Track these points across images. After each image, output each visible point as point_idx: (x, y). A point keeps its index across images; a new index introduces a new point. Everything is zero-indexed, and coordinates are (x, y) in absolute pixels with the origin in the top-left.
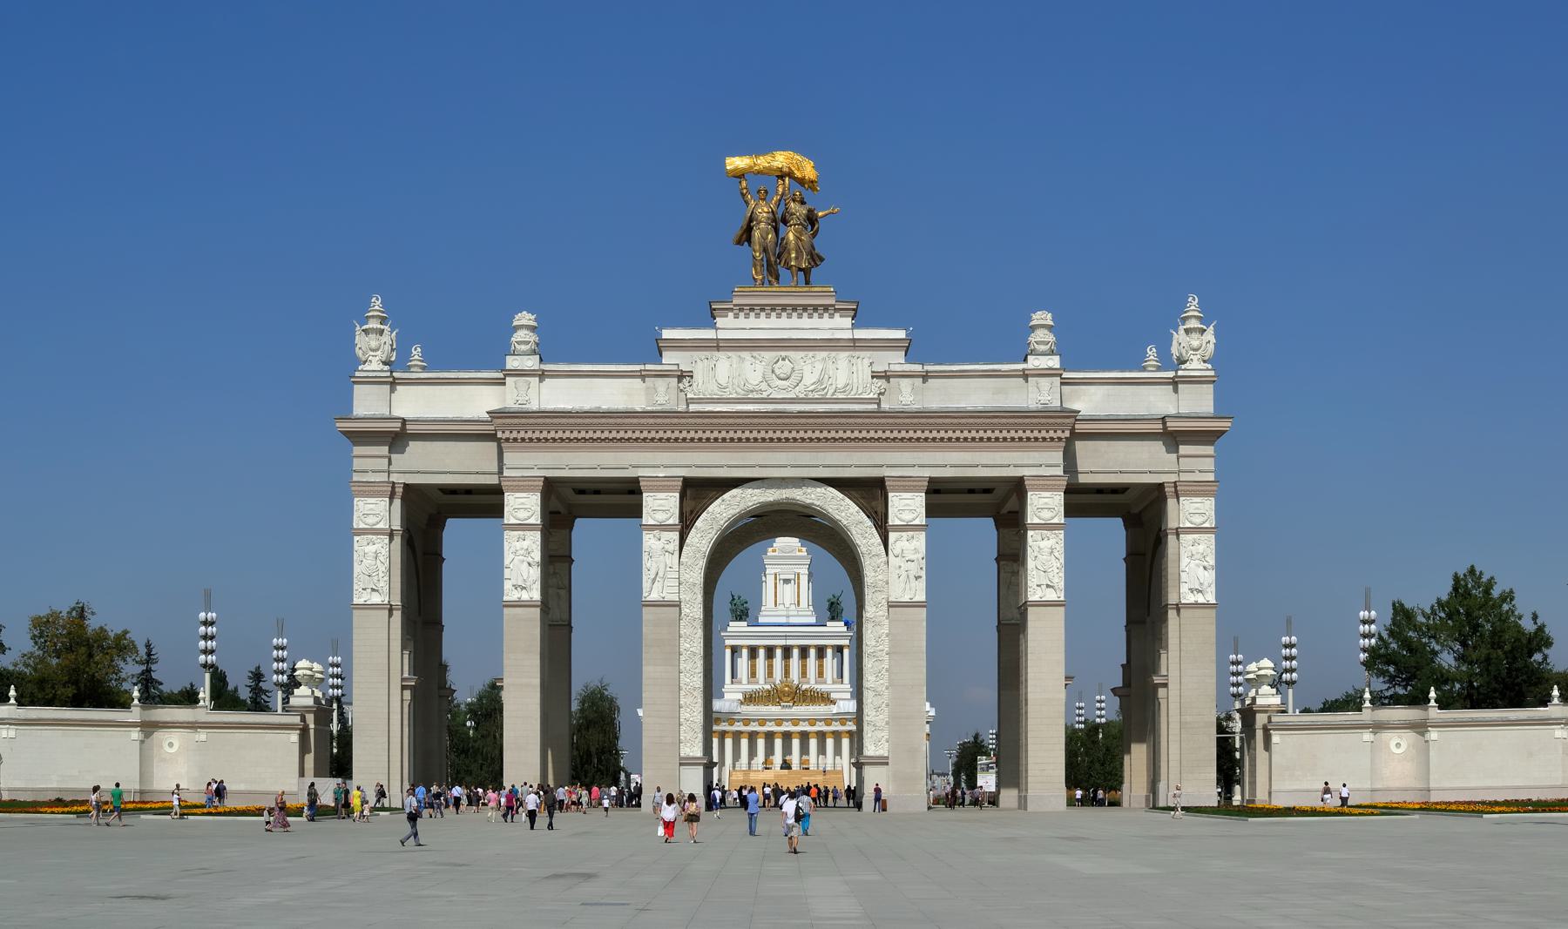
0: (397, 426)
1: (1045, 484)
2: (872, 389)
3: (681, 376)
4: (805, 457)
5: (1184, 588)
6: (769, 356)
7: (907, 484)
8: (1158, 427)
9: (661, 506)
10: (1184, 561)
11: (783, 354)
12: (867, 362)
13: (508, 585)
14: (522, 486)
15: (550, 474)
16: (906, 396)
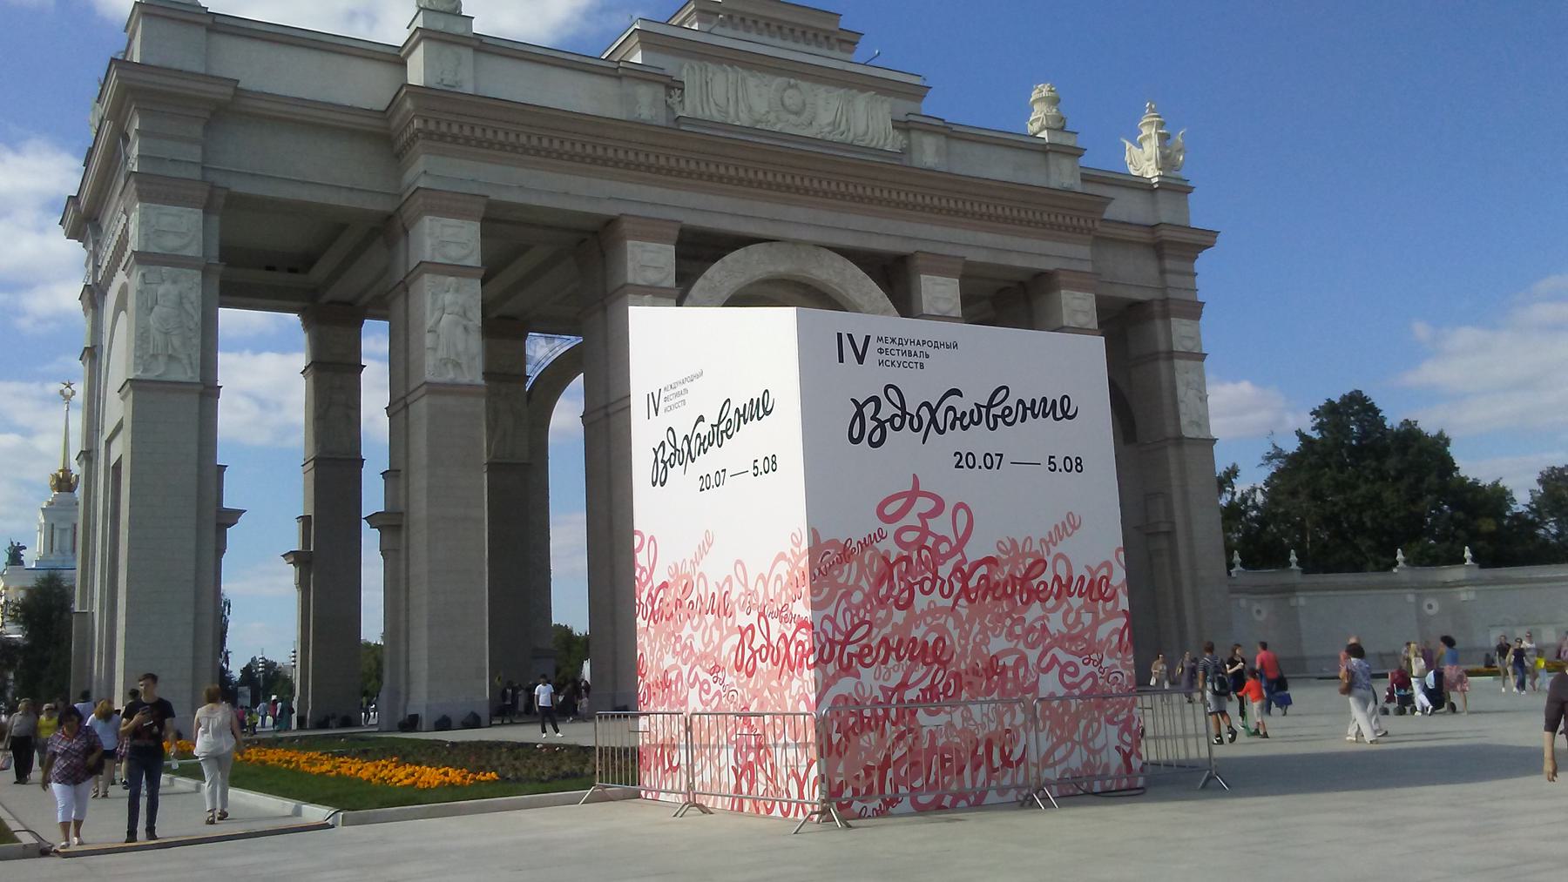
0: (223, 93)
1: (1080, 282)
2: (892, 141)
3: (673, 86)
4: (827, 217)
5: (1184, 421)
6: (780, 81)
7: (940, 265)
8: (1145, 236)
9: (650, 258)
10: (1181, 390)
11: (792, 81)
12: (887, 106)
13: (430, 361)
14: (449, 205)
15: (494, 196)
16: (929, 153)
